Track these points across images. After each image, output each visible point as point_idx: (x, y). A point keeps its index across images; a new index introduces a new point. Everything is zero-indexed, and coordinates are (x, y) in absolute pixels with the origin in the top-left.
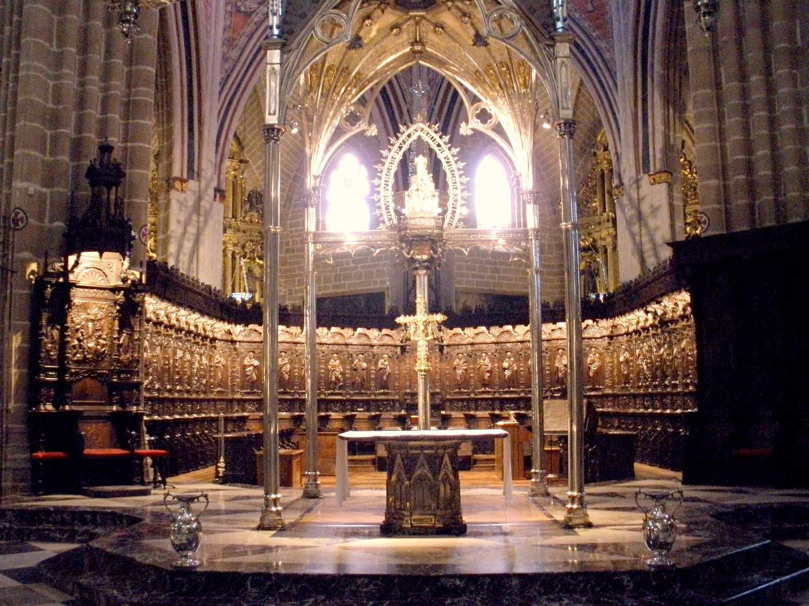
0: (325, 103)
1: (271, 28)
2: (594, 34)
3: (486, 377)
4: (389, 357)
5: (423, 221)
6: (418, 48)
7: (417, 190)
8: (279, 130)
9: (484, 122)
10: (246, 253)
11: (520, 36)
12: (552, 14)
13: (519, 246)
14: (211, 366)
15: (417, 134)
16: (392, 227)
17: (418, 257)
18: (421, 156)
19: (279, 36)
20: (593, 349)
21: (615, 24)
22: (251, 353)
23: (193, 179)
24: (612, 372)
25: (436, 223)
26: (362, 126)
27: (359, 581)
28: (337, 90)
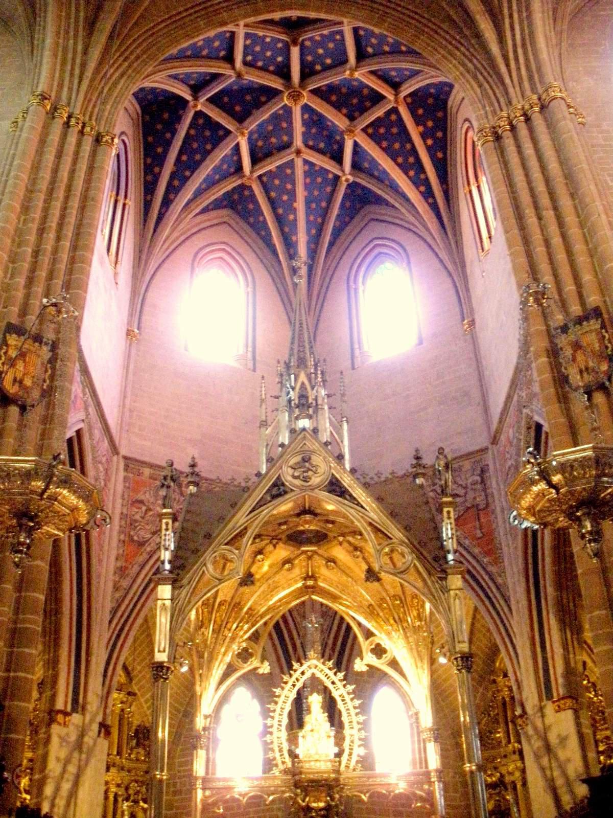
0: (217, 639)
1: (163, 562)
2: (485, 560)
5: (318, 764)
6: (310, 583)
7: (312, 731)
8: (168, 668)
11: (412, 570)
12: (442, 547)
13: (422, 790)
16: (285, 772)
17: (314, 805)
18: (315, 695)
19: (171, 572)
21: (505, 549)
23: (77, 712)
25: (333, 766)
26: (254, 663)
28: (229, 626)
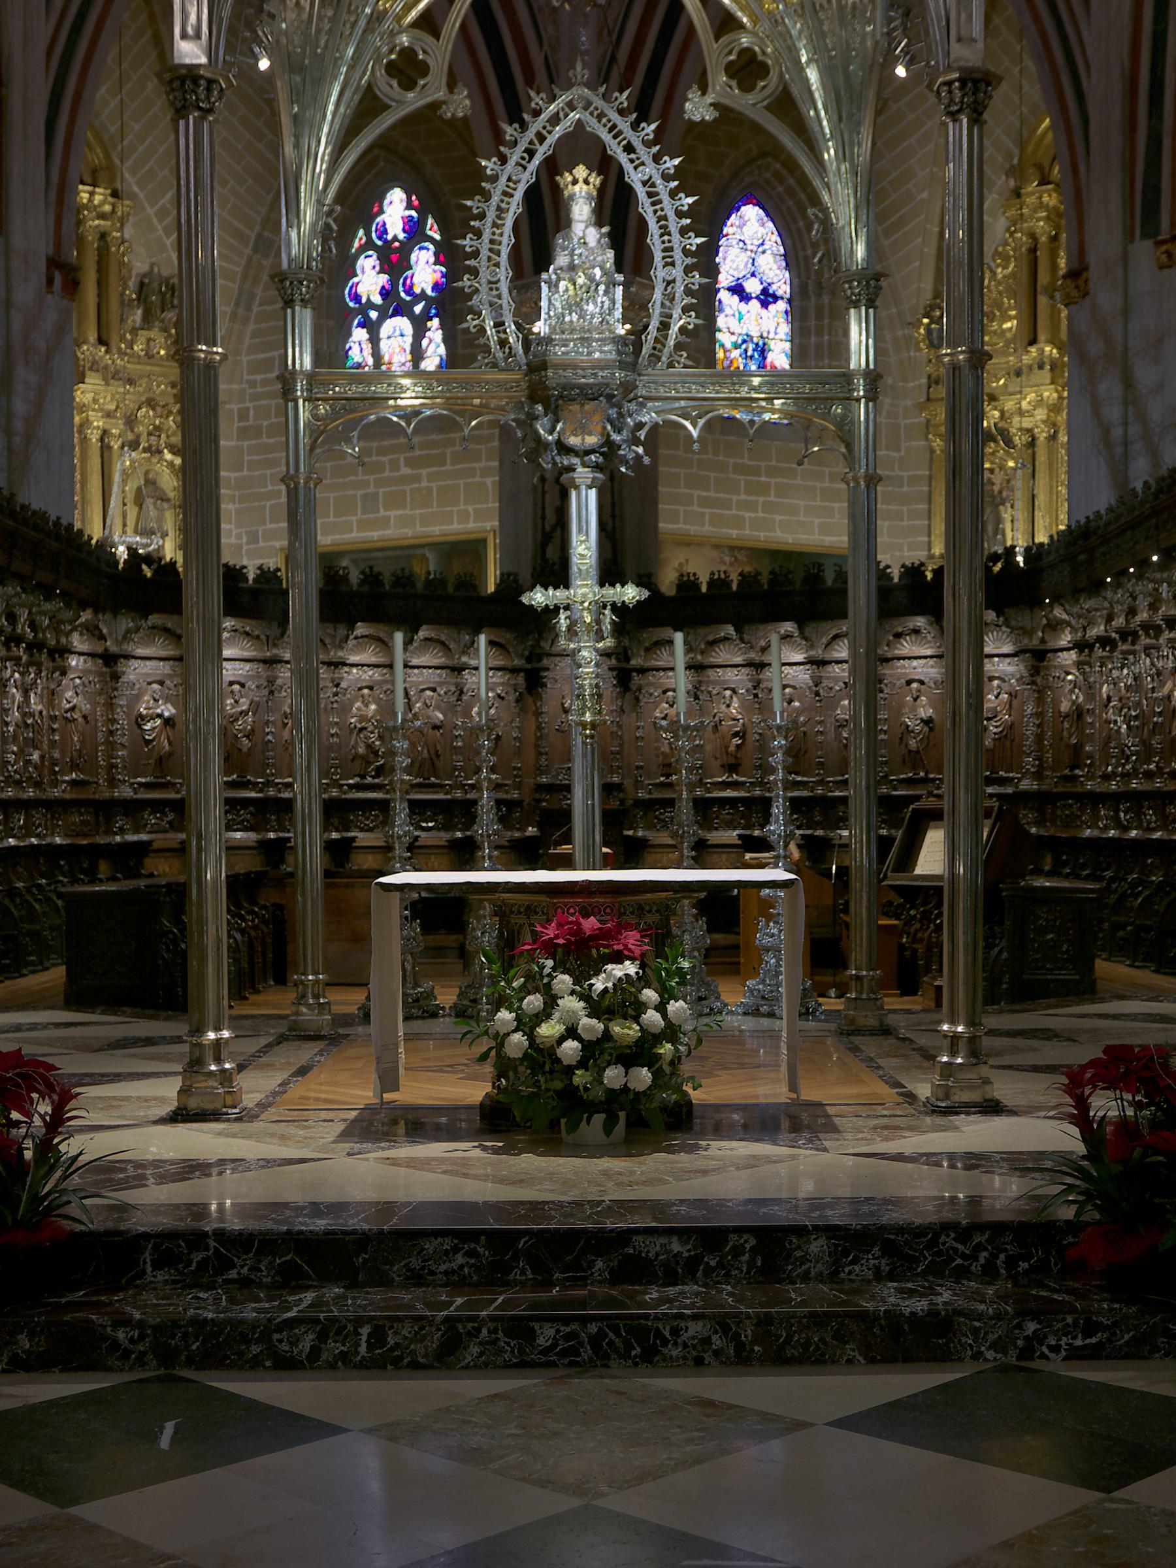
3: (732, 748)
4: (499, 696)
7: (572, 268)
8: (211, 82)
9: (747, 86)
10: (138, 436)
14: (54, 718)
15: (574, 116)
20: (996, 682)
22: (156, 686)
24: (1039, 738)
25: (619, 353)
27: (430, 1246)
